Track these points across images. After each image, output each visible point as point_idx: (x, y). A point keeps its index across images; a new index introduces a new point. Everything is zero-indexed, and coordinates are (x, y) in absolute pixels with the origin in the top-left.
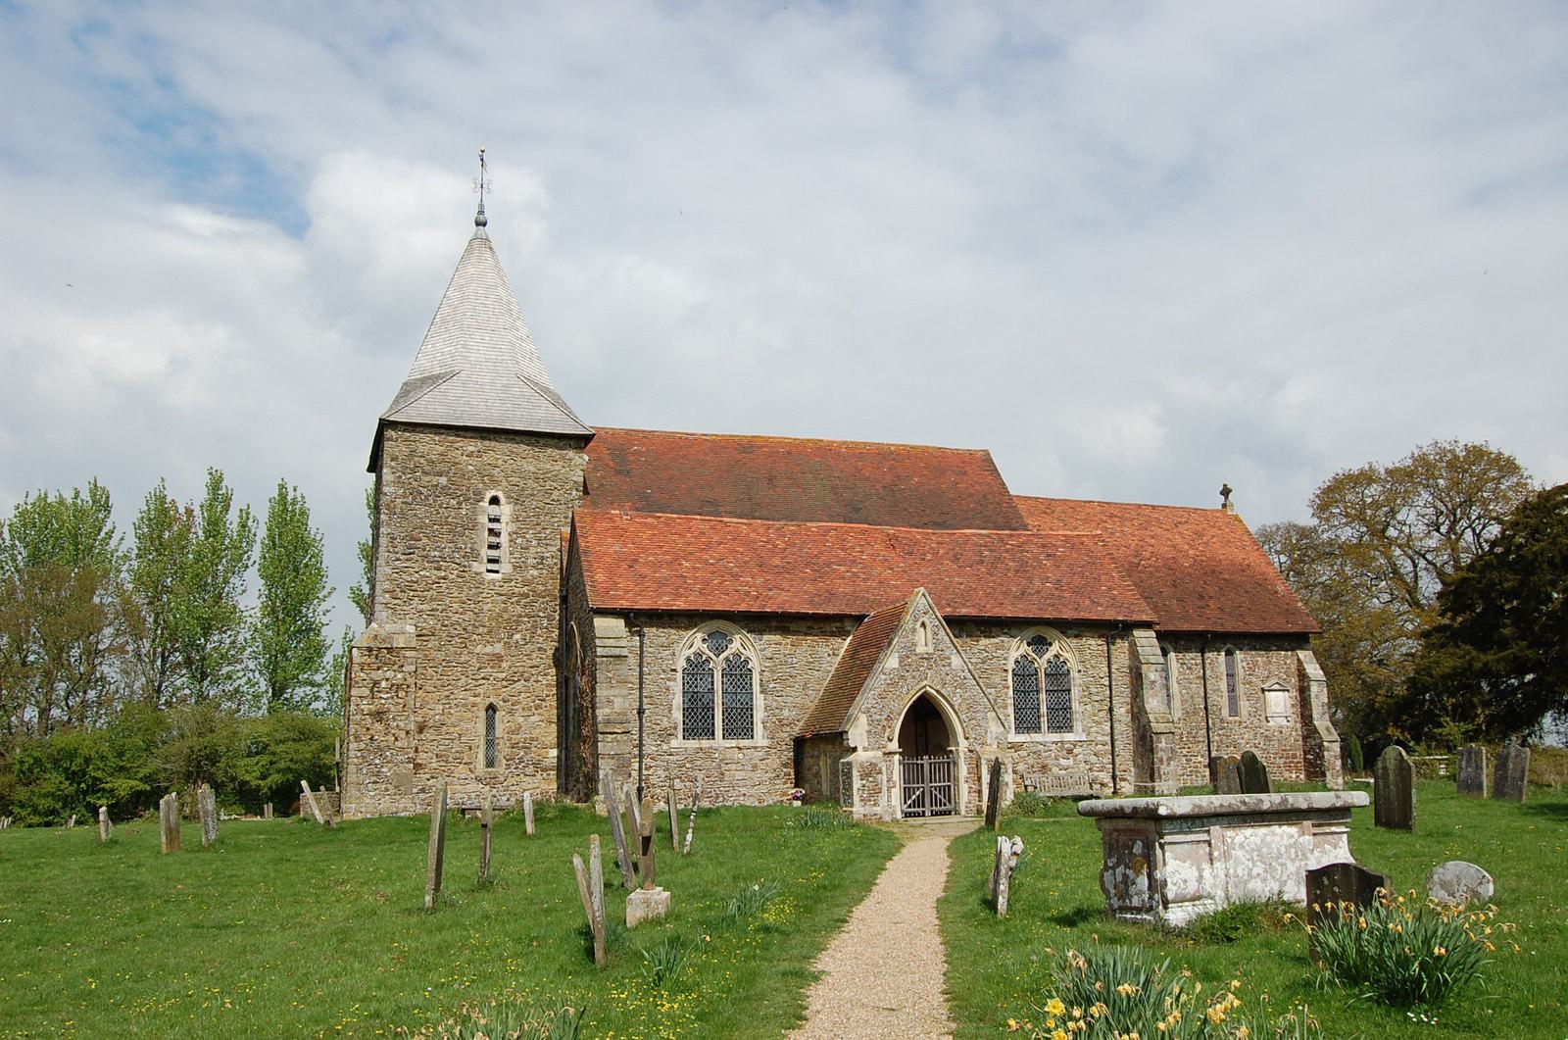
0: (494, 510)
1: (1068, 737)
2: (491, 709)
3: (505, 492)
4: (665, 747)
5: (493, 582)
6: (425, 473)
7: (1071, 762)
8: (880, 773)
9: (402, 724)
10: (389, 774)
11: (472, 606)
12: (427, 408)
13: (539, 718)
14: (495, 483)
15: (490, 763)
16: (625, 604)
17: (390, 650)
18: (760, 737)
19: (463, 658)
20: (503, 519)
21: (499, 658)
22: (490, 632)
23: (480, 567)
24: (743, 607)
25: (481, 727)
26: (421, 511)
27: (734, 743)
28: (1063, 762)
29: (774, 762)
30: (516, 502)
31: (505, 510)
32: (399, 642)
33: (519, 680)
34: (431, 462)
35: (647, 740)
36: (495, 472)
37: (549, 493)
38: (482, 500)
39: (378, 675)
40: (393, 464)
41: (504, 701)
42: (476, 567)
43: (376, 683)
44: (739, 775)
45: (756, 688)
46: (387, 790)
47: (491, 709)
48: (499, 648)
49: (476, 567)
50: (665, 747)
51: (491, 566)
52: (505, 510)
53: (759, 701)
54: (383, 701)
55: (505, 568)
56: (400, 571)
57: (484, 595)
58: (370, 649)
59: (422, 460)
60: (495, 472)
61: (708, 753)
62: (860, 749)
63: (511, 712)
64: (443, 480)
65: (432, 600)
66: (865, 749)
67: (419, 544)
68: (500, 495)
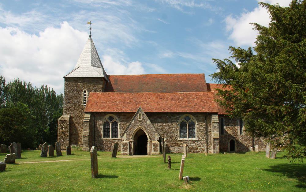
0: (85, 94)
1: (194, 139)
3: (87, 90)
4: (100, 139)
7: (194, 145)
8: (127, 145)
14: (85, 88)
16: (91, 111)
17: (64, 120)
19: (79, 122)
24: (115, 111)
27: (114, 139)
28: (192, 145)
35: (96, 138)
42: (82, 104)
45: (119, 127)
49: (82, 104)
50: (100, 139)
52: (87, 93)
60: (85, 86)
61: (109, 141)
62: (124, 140)
66: (125, 140)
67: (70, 100)
68: (86, 90)
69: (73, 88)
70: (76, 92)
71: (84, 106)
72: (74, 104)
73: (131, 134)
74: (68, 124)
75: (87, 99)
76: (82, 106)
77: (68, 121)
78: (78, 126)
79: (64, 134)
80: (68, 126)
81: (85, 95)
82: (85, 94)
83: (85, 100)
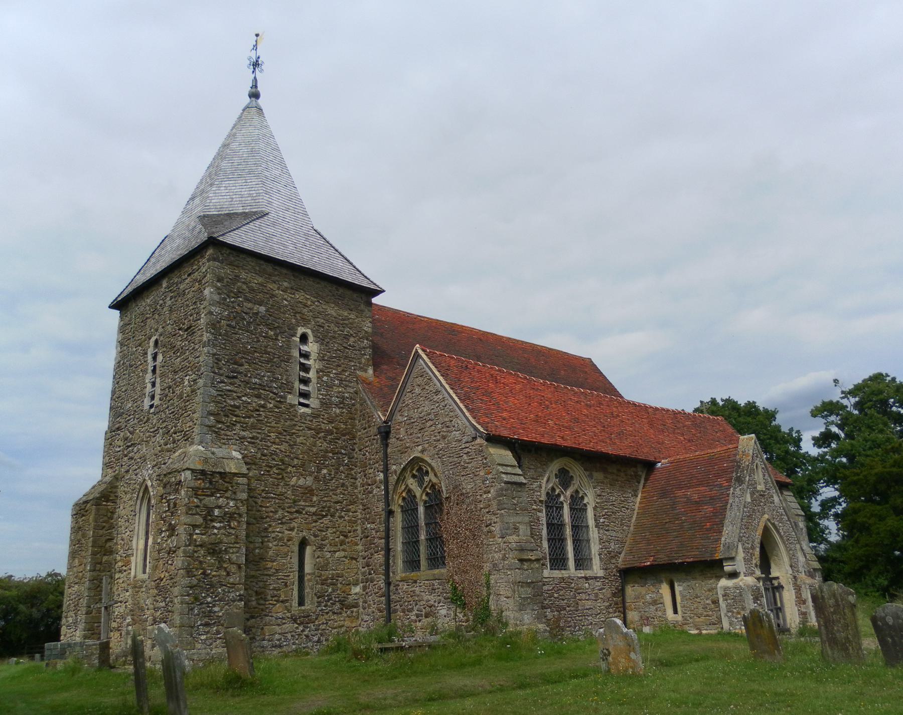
0: (305, 348)
2: (303, 544)
5: (304, 415)
6: (247, 300)
9: (234, 557)
10: (220, 614)
11: (288, 437)
12: (241, 237)
13: (342, 554)
14: (305, 322)
15: (301, 603)
17: (223, 475)
18: (597, 568)
20: (314, 356)
21: (309, 492)
22: (303, 465)
23: (293, 399)
25: (295, 561)
26: (244, 337)
29: (607, 592)
30: (320, 340)
31: (312, 347)
32: (232, 468)
33: (327, 515)
34: (252, 290)
36: (305, 311)
37: (347, 337)
38: (294, 335)
39: (210, 501)
40: (219, 284)
41: (315, 536)
43: (210, 510)
44: (588, 604)
45: (591, 522)
46: (218, 632)
47: (303, 544)
48: (309, 481)
49: (293, 399)
51: (302, 400)
52: (312, 347)
53: (594, 534)
54: (216, 531)
55: (314, 402)
56: (224, 394)
57: (298, 428)
58: (203, 472)
59: (244, 287)
60: (305, 311)
63: (321, 547)
64: (262, 309)
65: (253, 427)
67: (241, 369)
68: (309, 332)
69: (250, 305)
70: (265, 329)
71: (303, 410)
72: (258, 391)
73: (753, 548)
74: (244, 496)
75: (312, 375)
76: (292, 406)
77: (245, 480)
78: (276, 512)
79: (221, 561)
80: (243, 509)
81: (306, 356)
82: (305, 348)
83: (305, 381)
